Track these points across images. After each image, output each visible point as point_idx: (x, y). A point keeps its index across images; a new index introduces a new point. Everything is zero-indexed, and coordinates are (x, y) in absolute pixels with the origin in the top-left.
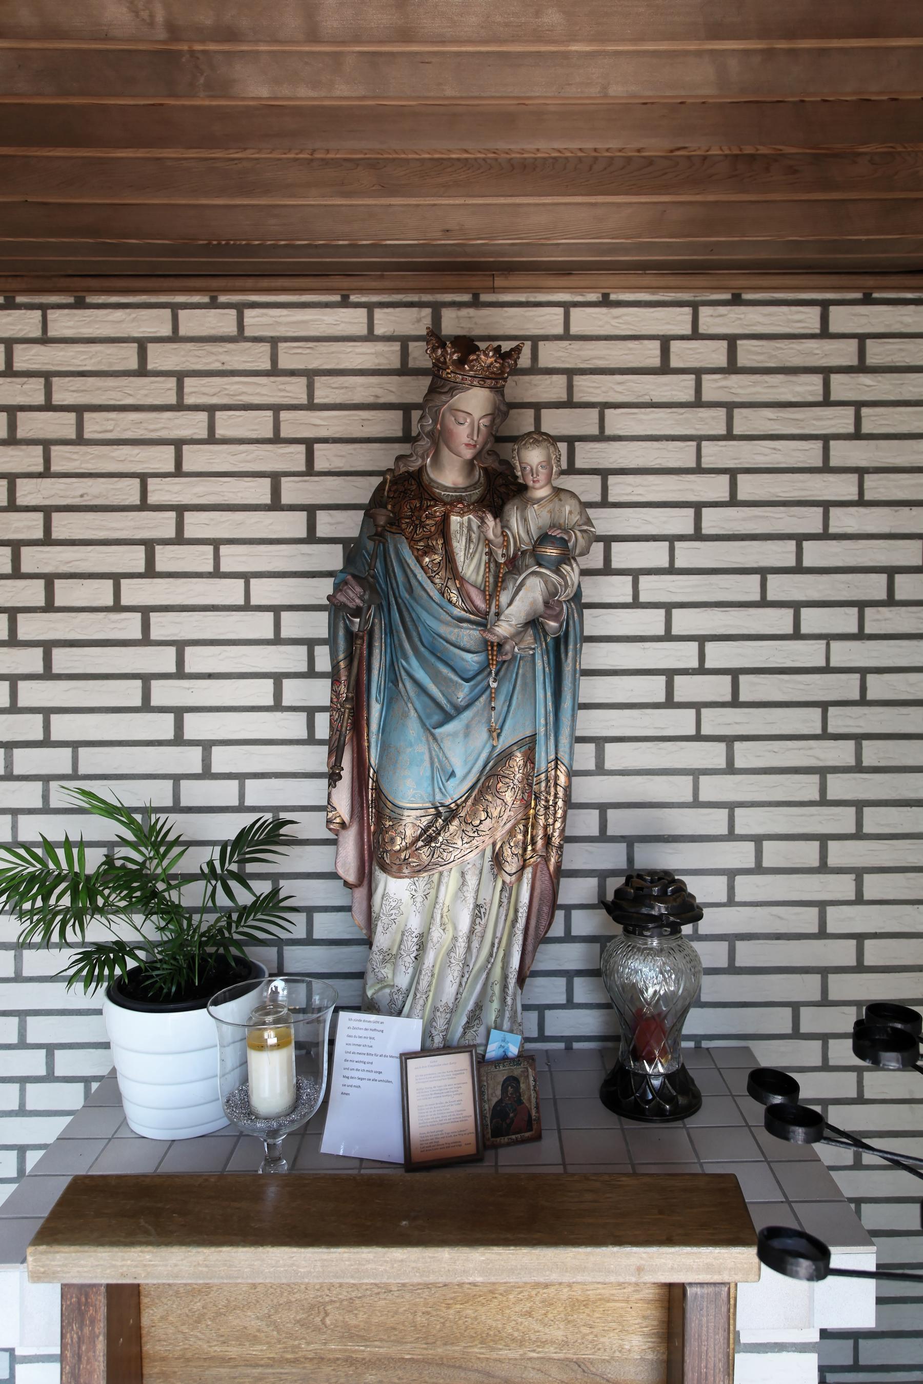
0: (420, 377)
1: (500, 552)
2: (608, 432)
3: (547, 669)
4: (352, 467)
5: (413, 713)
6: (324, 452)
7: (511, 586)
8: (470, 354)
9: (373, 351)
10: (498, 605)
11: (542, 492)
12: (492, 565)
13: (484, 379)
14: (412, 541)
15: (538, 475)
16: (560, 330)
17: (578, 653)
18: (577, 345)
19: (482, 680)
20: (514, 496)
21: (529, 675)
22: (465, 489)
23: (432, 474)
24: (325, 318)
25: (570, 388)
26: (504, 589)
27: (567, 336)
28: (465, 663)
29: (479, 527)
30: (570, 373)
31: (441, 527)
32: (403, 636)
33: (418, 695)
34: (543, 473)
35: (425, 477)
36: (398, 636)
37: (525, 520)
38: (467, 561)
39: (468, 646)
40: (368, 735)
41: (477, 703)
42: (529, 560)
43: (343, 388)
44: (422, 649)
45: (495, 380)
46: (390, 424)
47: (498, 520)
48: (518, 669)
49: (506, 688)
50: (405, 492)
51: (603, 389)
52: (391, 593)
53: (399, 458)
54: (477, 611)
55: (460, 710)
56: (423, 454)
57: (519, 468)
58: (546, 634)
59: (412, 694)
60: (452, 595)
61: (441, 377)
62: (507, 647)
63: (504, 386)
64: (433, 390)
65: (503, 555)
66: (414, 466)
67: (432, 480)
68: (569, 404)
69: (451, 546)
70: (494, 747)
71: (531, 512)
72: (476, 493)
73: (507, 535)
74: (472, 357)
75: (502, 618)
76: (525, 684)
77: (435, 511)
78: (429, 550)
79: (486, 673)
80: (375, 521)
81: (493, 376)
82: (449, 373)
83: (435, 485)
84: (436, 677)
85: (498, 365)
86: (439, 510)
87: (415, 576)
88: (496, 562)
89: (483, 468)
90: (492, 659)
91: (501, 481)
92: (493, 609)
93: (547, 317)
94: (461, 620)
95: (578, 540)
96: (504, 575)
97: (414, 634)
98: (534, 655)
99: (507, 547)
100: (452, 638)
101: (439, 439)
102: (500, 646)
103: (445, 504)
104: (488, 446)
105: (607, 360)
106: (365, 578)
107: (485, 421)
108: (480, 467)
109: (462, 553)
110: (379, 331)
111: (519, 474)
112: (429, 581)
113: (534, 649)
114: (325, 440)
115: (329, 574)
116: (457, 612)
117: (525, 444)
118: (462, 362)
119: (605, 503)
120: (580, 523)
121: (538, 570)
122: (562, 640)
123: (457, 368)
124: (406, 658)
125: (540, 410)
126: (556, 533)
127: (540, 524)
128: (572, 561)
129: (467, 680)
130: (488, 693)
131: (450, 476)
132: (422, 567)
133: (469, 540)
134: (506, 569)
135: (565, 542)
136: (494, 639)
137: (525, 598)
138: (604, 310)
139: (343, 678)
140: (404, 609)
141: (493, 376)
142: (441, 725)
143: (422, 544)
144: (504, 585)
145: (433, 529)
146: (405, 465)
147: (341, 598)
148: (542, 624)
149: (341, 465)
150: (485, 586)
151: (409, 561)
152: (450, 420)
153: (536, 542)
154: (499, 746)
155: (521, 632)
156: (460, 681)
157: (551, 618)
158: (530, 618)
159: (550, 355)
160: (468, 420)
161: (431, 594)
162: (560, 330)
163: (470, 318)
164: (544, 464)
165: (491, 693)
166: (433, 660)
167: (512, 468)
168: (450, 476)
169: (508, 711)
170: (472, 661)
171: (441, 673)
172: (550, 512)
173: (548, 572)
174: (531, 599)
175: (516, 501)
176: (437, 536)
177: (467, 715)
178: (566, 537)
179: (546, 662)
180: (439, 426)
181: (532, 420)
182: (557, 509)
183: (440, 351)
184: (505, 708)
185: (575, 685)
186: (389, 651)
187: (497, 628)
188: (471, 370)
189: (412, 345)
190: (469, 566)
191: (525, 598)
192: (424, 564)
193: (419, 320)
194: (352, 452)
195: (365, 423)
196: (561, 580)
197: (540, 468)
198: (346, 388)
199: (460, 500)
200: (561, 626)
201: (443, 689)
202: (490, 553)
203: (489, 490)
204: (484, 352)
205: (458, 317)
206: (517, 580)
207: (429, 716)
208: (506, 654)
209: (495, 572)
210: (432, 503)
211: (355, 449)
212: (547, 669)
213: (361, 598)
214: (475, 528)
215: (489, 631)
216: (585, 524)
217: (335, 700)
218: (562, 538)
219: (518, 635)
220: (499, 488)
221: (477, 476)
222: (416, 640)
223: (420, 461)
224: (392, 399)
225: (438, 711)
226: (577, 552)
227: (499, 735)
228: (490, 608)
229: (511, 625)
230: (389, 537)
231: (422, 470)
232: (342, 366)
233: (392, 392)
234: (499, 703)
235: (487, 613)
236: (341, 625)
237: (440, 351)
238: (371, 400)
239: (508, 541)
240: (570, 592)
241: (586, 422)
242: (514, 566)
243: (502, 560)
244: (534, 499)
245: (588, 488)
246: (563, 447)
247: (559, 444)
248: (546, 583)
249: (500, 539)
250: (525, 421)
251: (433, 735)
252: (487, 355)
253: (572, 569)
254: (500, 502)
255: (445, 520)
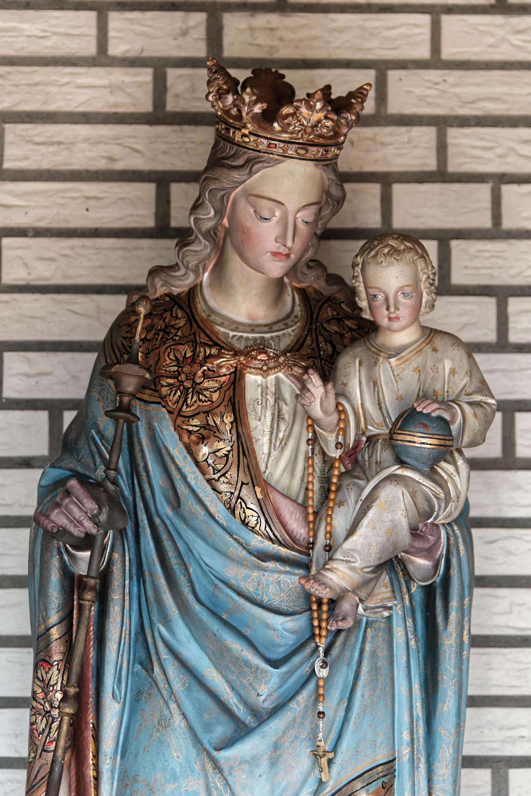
0: (186, 128)
1: (331, 438)
2: (507, 224)
3: (412, 643)
4: (66, 277)
5: (178, 720)
6: (20, 253)
7: (352, 499)
8: (282, 105)
9: (105, 82)
10: (330, 533)
11: (403, 336)
12: (318, 460)
13: (305, 145)
14: (177, 415)
15: (397, 309)
16: (423, 52)
17: (465, 612)
18: (454, 76)
19: (302, 663)
20: (353, 340)
21: (383, 653)
22: (270, 327)
23: (212, 300)
24: (25, 26)
25: (442, 147)
26: (341, 504)
27: (435, 62)
28: (271, 632)
29: (297, 396)
30: (442, 123)
31: (229, 394)
32: (162, 582)
33: (188, 689)
34: (405, 305)
35: (200, 306)
36: (153, 582)
37: (375, 384)
38: (274, 453)
39: (276, 602)
40: (96, 756)
41: (293, 705)
42: (383, 454)
43: (52, 144)
44: (197, 607)
45: (323, 148)
46: (135, 205)
47: (330, 386)
48: (363, 642)
49: (344, 676)
50: (166, 330)
51: (499, 151)
52: (140, 505)
53: (155, 272)
54: (292, 542)
55: (262, 717)
56: (197, 266)
57: (363, 295)
58: (409, 578)
59: (177, 686)
60: (249, 512)
61: (231, 142)
62: (346, 606)
63: (337, 156)
64: (217, 161)
65: (338, 445)
66: (180, 285)
67: (213, 311)
68: (441, 175)
69: (246, 426)
70: (321, 783)
71: (385, 370)
72: (288, 335)
73: (344, 411)
74: (286, 110)
75: (338, 555)
76: (375, 670)
77: (220, 366)
78: (208, 433)
79: (308, 650)
80: (117, 384)
81: (321, 141)
82: (246, 134)
83: (219, 320)
84: (220, 656)
85: (329, 124)
86: (225, 364)
87: (184, 477)
88: (324, 454)
89: (302, 292)
90: (320, 627)
91: (329, 312)
92: (321, 540)
93: (403, 30)
94: (264, 556)
95: (465, 419)
96: (341, 476)
97: (182, 580)
98: (389, 618)
99: (345, 431)
100: (249, 588)
101: (226, 241)
102: (333, 603)
103: (236, 353)
104: (309, 254)
105: (504, 102)
106: (99, 484)
107: (308, 215)
108: (294, 288)
109: (266, 439)
110: (116, 49)
111: (363, 304)
112: (209, 488)
113: (390, 608)
114: (21, 232)
115: (26, 463)
116: (258, 542)
117: (375, 256)
118: (268, 117)
119: (502, 345)
120: (469, 390)
121: (399, 472)
122: (439, 591)
123: (260, 127)
124: (166, 621)
125: (390, 185)
126: (430, 409)
127: (401, 392)
128: (456, 455)
129: (275, 664)
130: (311, 686)
131: (242, 304)
132: (197, 463)
133: (278, 416)
134: (344, 470)
135: (444, 424)
136: (325, 594)
137: (379, 520)
138: (498, 19)
139: (56, 657)
140: (164, 537)
141: (321, 141)
142: (228, 743)
143: (196, 422)
144: (340, 497)
145: (215, 396)
146: (166, 284)
147: (58, 518)
148: (401, 562)
149: (48, 274)
150: (306, 497)
151: (175, 452)
152: (246, 212)
153: (395, 424)
154: (331, 783)
155: (371, 580)
156: (264, 665)
157: (418, 552)
158: (386, 557)
159: (407, 93)
160: (277, 213)
161: (212, 510)
162: (423, 52)
163: (272, 29)
164: (408, 290)
165: (318, 686)
166: (215, 626)
167: (353, 292)
168: (242, 304)
169: (346, 719)
170: (284, 629)
171: (229, 650)
172: (418, 370)
173: (416, 476)
174: (388, 524)
175: (358, 350)
176: (222, 408)
177: (276, 725)
178: (447, 416)
179: (410, 629)
180: (225, 222)
181: (376, 203)
182: (429, 364)
183: (230, 99)
184: (341, 713)
185: (460, 670)
186: (135, 607)
187: (329, 574)
188: (284, 131)
189: (172, 74)
190: (278, 460)
191: (379, 520)
192: (201, 458)
193: (184, 33)
194: (67, 252)
195: (92, 203)
196: (439, 490)
197: (400, 297)
198: (59, 143)
199: (261, 347)
200: (436, 566)
201: (233, 677)
202: (314, 440)
203: (310, 330)
204: (307, 103)
205: (252, 29)
206: (362, 489)
207: (208, 728)
208: (344, 619)
209: (323, 471)
210: (214, 351)
211: (72, 248)
212: (412, 643)
213: (94, 519)
214: (287, 395)
215: (316, 579)
216: (478, 391)
217: (41, 696)
218: (440, 419)
219: (366, 585)
220: (328, 328)
221: (289, 304)
222: (186, 590)
223: (192, 277)
224: (139, 163)
225: (224, 718)
226: (466, 440)
227: (330, 762)
228: (315, 536)
229: (353, 569)
230: (138, 409)
231: (193, 292)
232: (52, 107)
233: (137, 151)
234: (332, 705)
235: (311, 545)
236: (55, 562)
237: (230, 99)
238: (101, 165)
239: (346, 421)
240: (454, 509)
241: (470, 207)
242: (356, 462)
243: (336, 454)
244: (389, 349)
245: (473, 318)
246: (431, 247)
247: (425, 243)
248: (413, 495)
249: (334, 418)
250: (364, 207)
251: (217, 766)
252: (311, 108)
253: (457, 470)
254: (330, 349)
255: (236, 380)
